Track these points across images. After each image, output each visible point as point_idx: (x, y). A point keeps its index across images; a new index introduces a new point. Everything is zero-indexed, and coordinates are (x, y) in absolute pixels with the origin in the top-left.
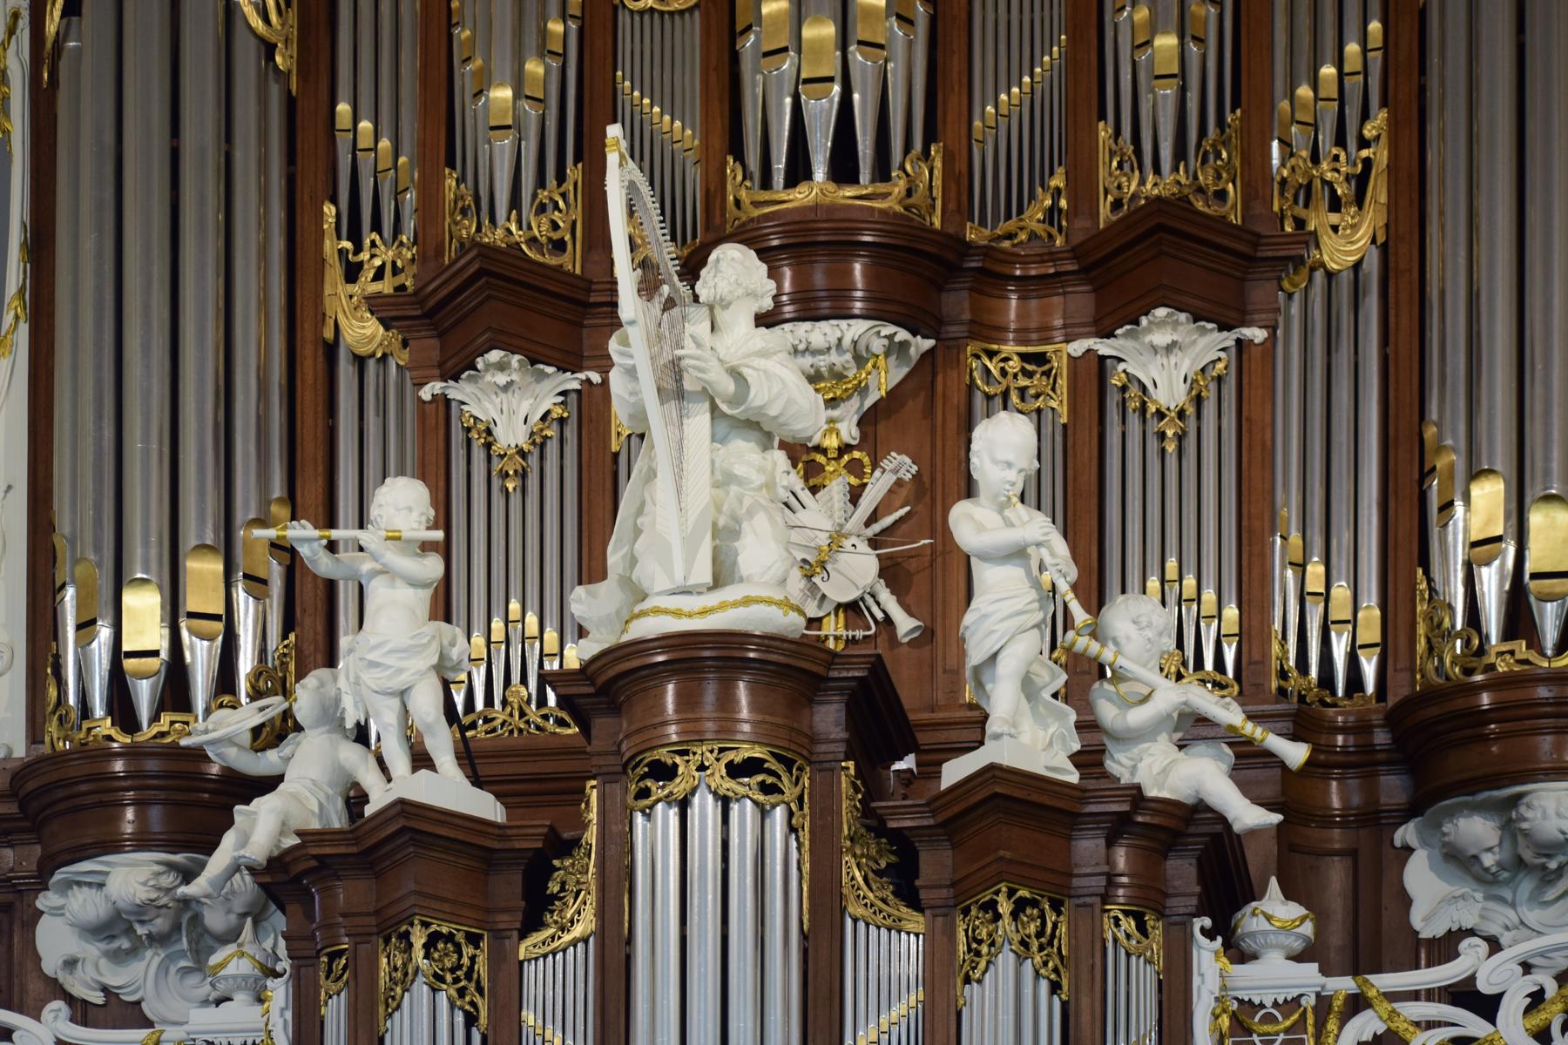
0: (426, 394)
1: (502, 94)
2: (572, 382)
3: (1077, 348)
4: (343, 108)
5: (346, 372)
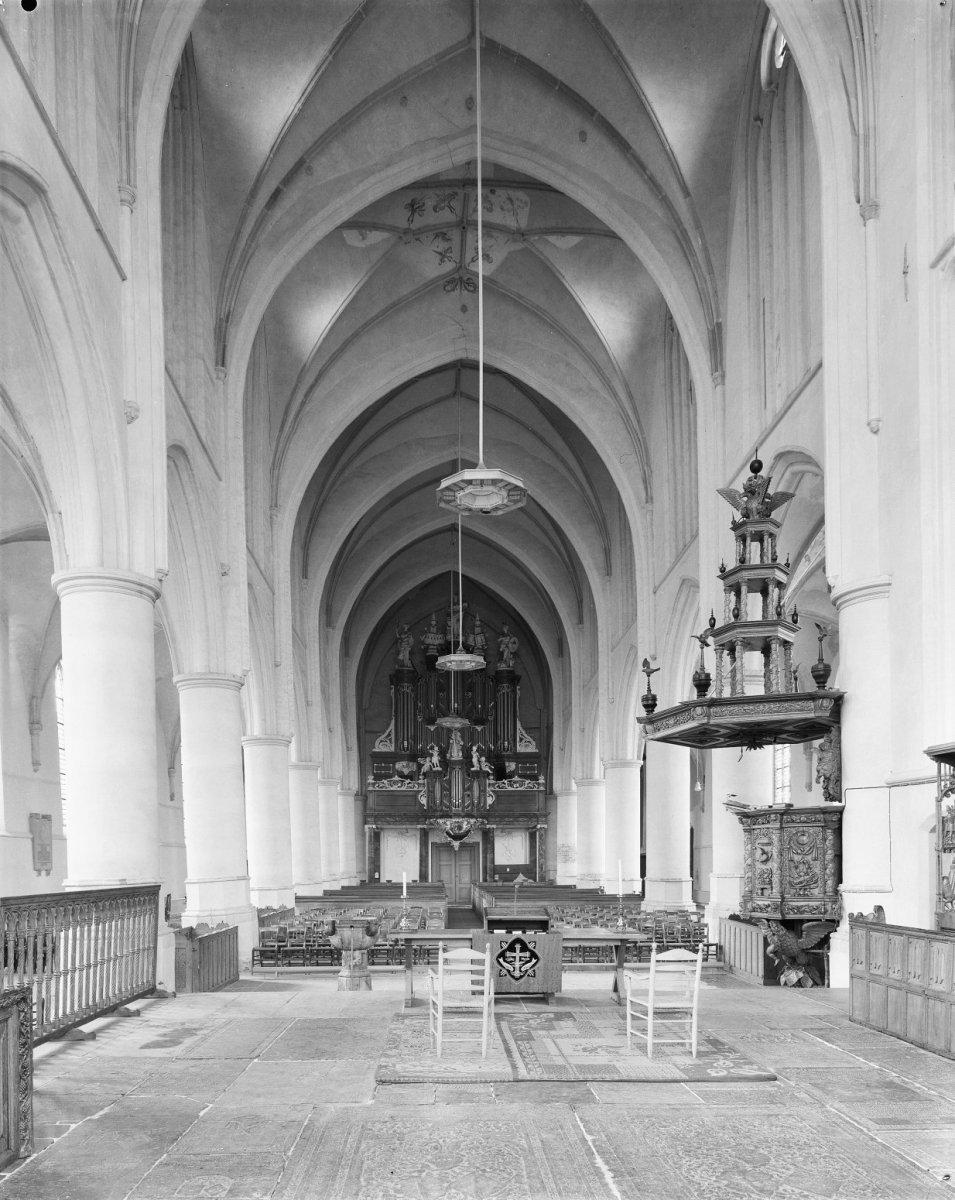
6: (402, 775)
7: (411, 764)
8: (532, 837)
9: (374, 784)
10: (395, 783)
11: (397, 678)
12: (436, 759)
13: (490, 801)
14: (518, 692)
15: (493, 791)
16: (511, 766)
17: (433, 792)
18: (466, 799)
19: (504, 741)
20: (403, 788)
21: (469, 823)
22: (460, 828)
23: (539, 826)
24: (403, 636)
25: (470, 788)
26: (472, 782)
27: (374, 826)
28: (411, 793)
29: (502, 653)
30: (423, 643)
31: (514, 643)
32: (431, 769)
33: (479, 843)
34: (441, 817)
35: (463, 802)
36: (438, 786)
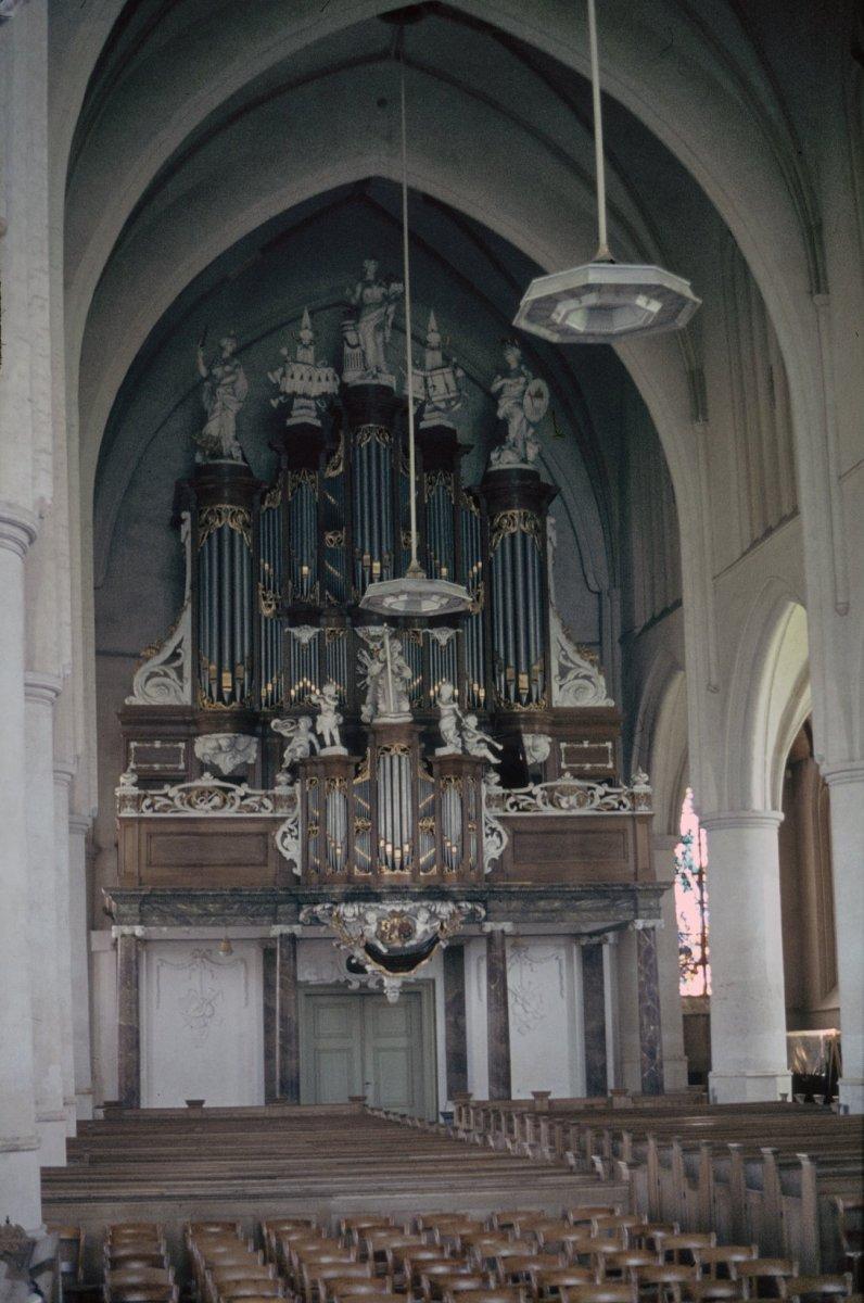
0: (286, 630)
1: (305, 569)
2: (317, 630)
3: (424, 631)
4: (262, 560)
5: (263, 620)
6: (217, 773)
7: (243, 740)
8: (591, 959)
9: (138, 800)
10: (205, 794)
11: (201, 486)
12: (329, 723)
13: (493, 848)
14: (551, 533)
15: (499, 819)
16: (538, 748)
17: (322, 822)
18: (424, 841)
19: (517, 672)
20: (229, 812)
21: (434, 915)
22: (407, 931)
23: (640, 924)
24: (218, 371)
25: (435, 810)
26: (440, 793)
27: (139, 931)
28: (253, 828)
29: (503, 425)
30: (276, 390)
31: (539, 395)
32: (313, 751)
33: (433, 981)
34: (350, 898)
35: (415, 852)
36: (336, 802)
